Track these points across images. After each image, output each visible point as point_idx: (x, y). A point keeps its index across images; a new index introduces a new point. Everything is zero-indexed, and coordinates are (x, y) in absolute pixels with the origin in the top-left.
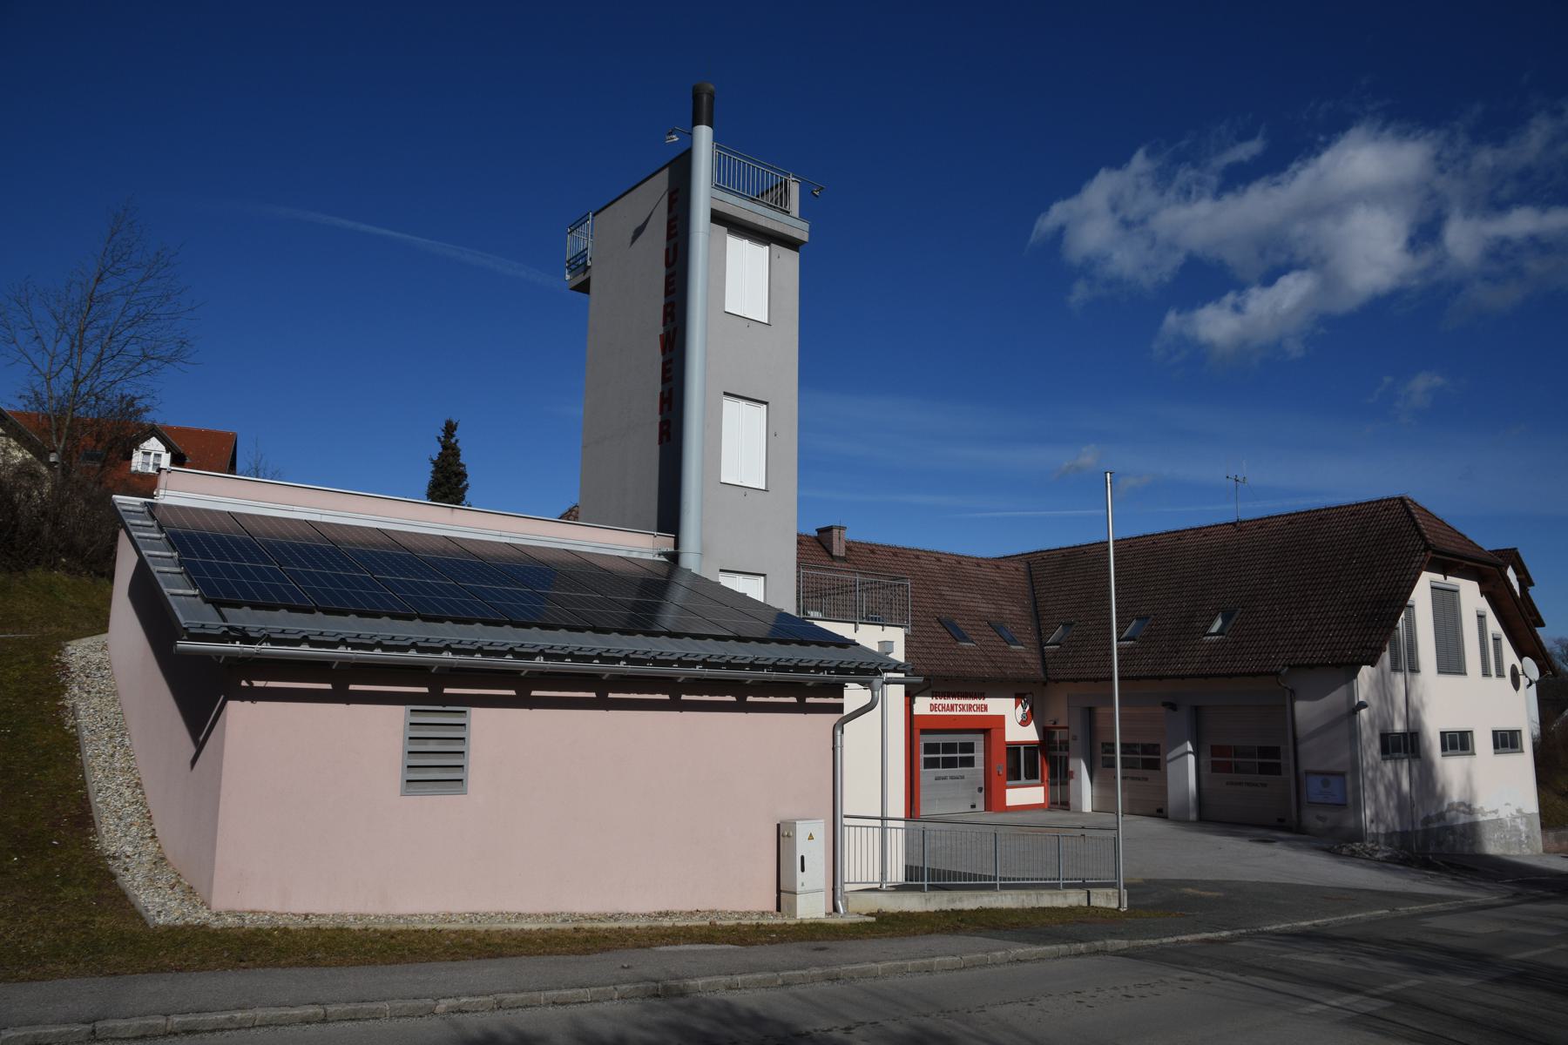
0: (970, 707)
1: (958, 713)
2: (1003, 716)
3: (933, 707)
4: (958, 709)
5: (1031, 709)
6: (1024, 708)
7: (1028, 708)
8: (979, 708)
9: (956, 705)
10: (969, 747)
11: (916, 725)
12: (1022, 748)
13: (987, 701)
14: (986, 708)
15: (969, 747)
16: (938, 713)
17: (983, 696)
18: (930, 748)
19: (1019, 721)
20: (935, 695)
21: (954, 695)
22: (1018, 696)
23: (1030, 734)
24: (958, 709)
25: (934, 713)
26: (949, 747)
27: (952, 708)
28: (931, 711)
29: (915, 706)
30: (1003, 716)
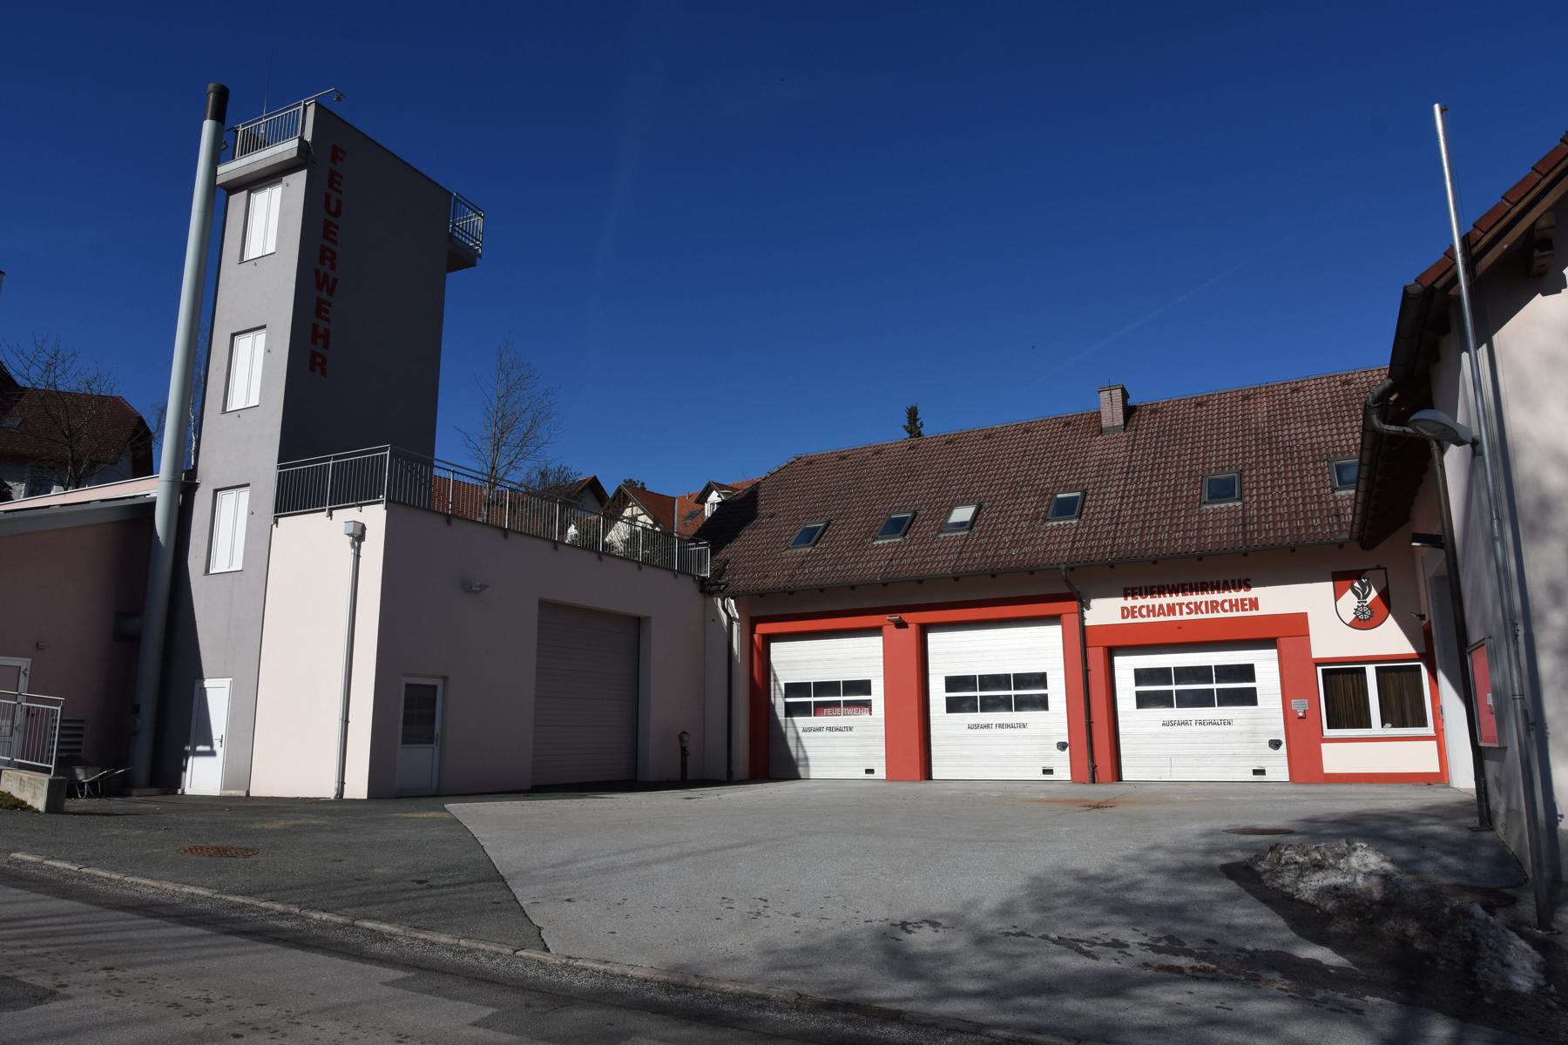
0: (1214, 606)
1: (1185, 617)
2: (1305, 615)
3: (1130, 612)
4: (1185, 610)
5: (1384, 596)
6: (1361, 596)
7: (1374, 594)
8: (1234, 605)
9: (1180, 605)
10: (1247, 672)
11: (1090, 642)
12: (1371, 671)
13: (1255, 592)
14: (1254, 604)
15: (1247, 672)
16: (1140, 620)
17: (1246, 584)
18: (1142, 676)
19: (1350, 617)
20: (1128, 593)
21: (1174, 590)
22: (1342, 578)
23: (1391, 640)
24: (1185, 610)
25: (1130, 620)
26: (1185, 674)
27: (1171, 609)
28: (1123, 617)
29: (1087, 613)
30: (1305, 615)
